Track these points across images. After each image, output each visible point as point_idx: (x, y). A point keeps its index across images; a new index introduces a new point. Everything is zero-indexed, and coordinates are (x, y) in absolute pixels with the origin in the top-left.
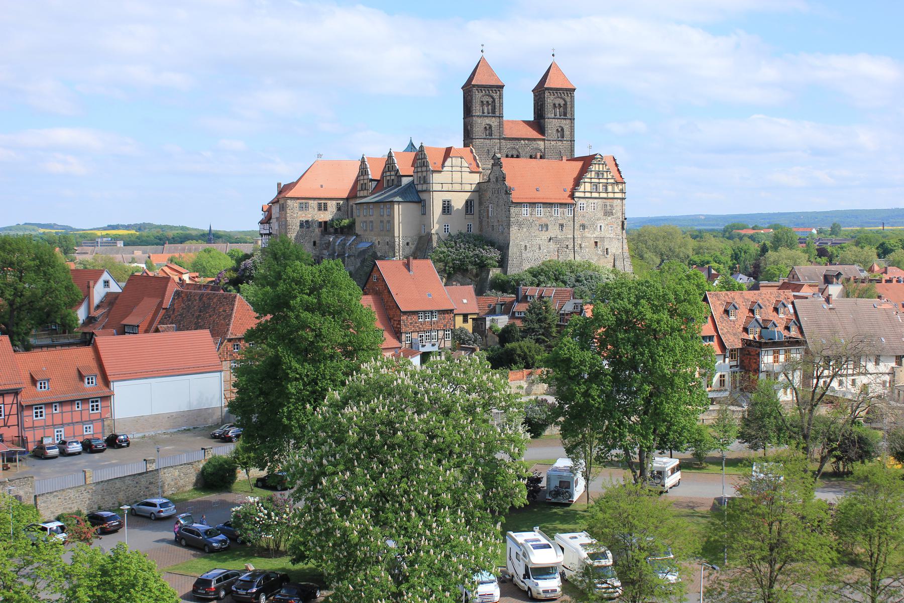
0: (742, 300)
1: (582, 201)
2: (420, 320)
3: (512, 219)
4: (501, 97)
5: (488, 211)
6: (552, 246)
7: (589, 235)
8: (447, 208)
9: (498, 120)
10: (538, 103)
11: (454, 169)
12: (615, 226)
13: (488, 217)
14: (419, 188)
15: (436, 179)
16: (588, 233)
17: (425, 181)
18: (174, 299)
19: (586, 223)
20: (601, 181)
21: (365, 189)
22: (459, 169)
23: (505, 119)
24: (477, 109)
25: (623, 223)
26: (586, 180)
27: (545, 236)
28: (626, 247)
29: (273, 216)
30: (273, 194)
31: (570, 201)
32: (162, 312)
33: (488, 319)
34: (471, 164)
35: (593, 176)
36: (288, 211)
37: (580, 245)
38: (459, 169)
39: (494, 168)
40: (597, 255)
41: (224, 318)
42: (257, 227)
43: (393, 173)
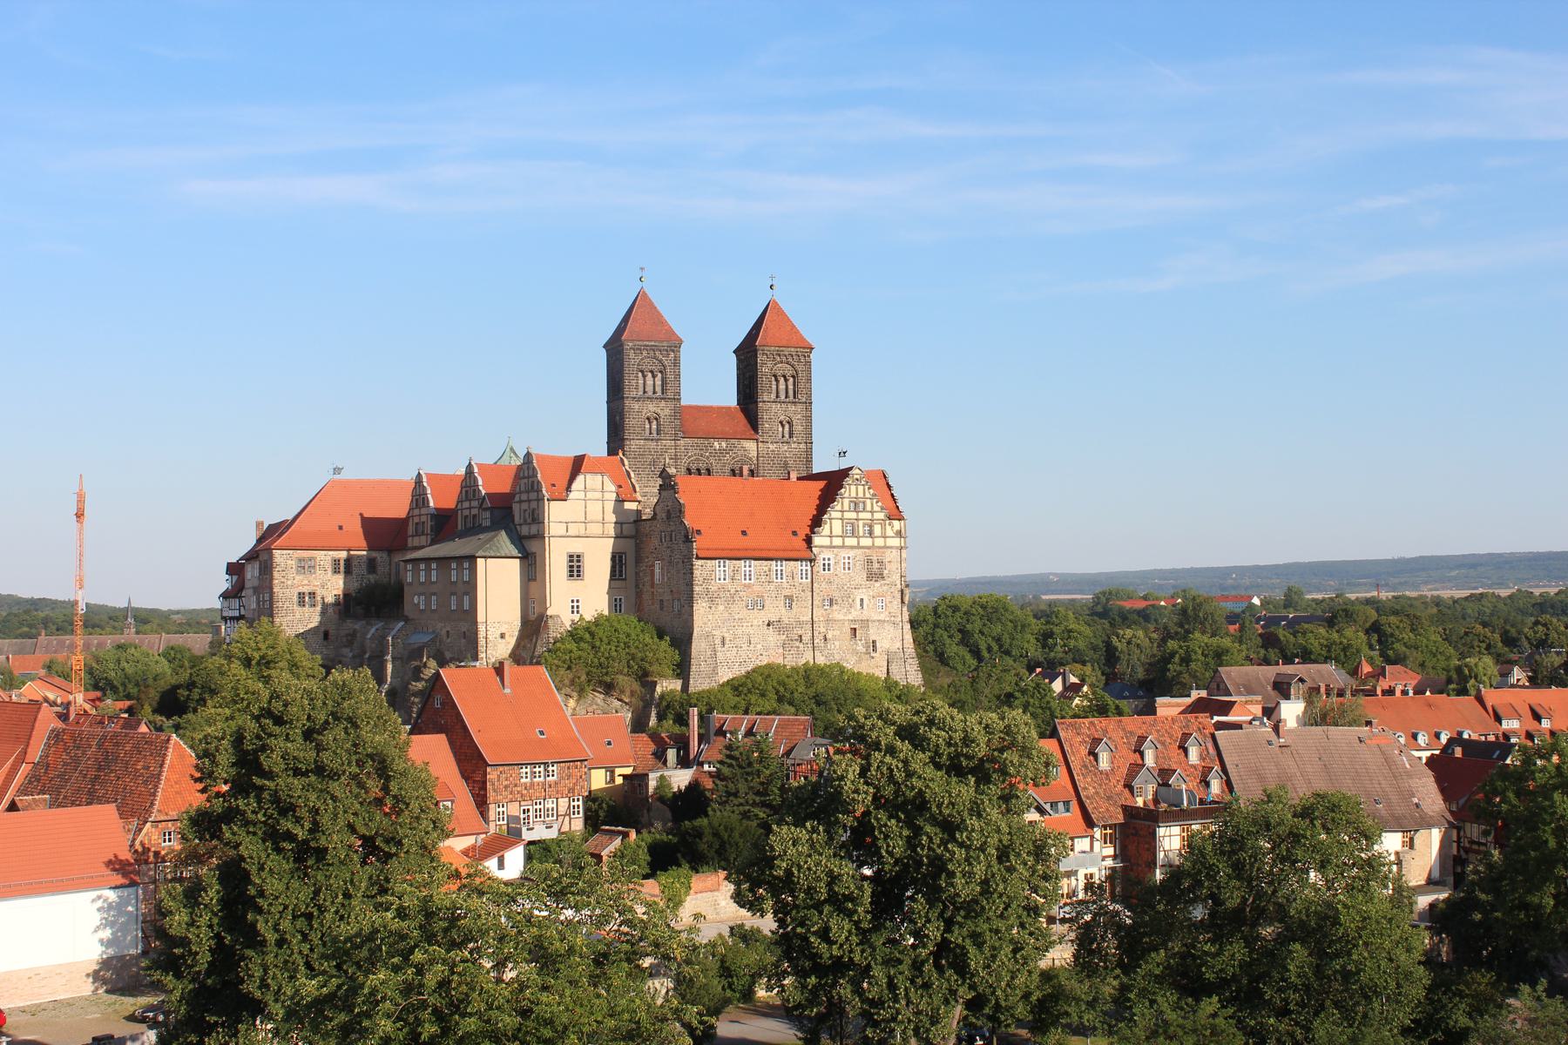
0: (1121, 733)
1: (826, 554)
2: (523, 780)
3: (697, 589)
4: (676, 363)
5: (653, 571)
6: (773, 638)
7: (841, 617)
8: (575, 567)
9: (671, 404)
10: (744, 374)
11: (590, 495)
12: (889, 599)
13: (653, 585)
14: (524, 530)
15: (556, 514)
16: (838, 613)
17: (537, 518)
18: (48, 745)
19: (836, 595)
20: (862, 515)
21: (423, 534)
22: (598, 495)
23: (683, 402)
24: (635, 384)
25: (902, 591)
26: (834, 514)
27: (760, 617)
28: (909, 637)
29: (248, 584)
30: (247, 542)
31: (807, 554)
32: (24, 769)
33: (651, 776)
34: (620, 487)
35: (846, 508)
36: (276, 574)
38: (598, 495)
39: (664, 493)
41: (145, 783)
42: (217, 604)
43: (475, 503)
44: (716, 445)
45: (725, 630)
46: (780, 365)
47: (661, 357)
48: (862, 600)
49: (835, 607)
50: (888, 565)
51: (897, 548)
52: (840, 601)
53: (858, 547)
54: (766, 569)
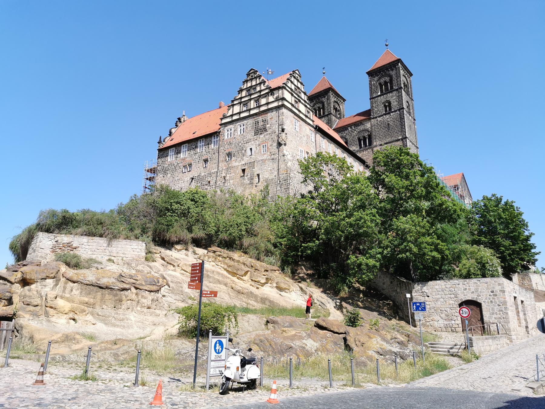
7: (237, 164)
19: (233, 150)
37: (225, 178)
48: (251, 149)
49: (233, 158)
50: (270, 123)
52: (236, 154)
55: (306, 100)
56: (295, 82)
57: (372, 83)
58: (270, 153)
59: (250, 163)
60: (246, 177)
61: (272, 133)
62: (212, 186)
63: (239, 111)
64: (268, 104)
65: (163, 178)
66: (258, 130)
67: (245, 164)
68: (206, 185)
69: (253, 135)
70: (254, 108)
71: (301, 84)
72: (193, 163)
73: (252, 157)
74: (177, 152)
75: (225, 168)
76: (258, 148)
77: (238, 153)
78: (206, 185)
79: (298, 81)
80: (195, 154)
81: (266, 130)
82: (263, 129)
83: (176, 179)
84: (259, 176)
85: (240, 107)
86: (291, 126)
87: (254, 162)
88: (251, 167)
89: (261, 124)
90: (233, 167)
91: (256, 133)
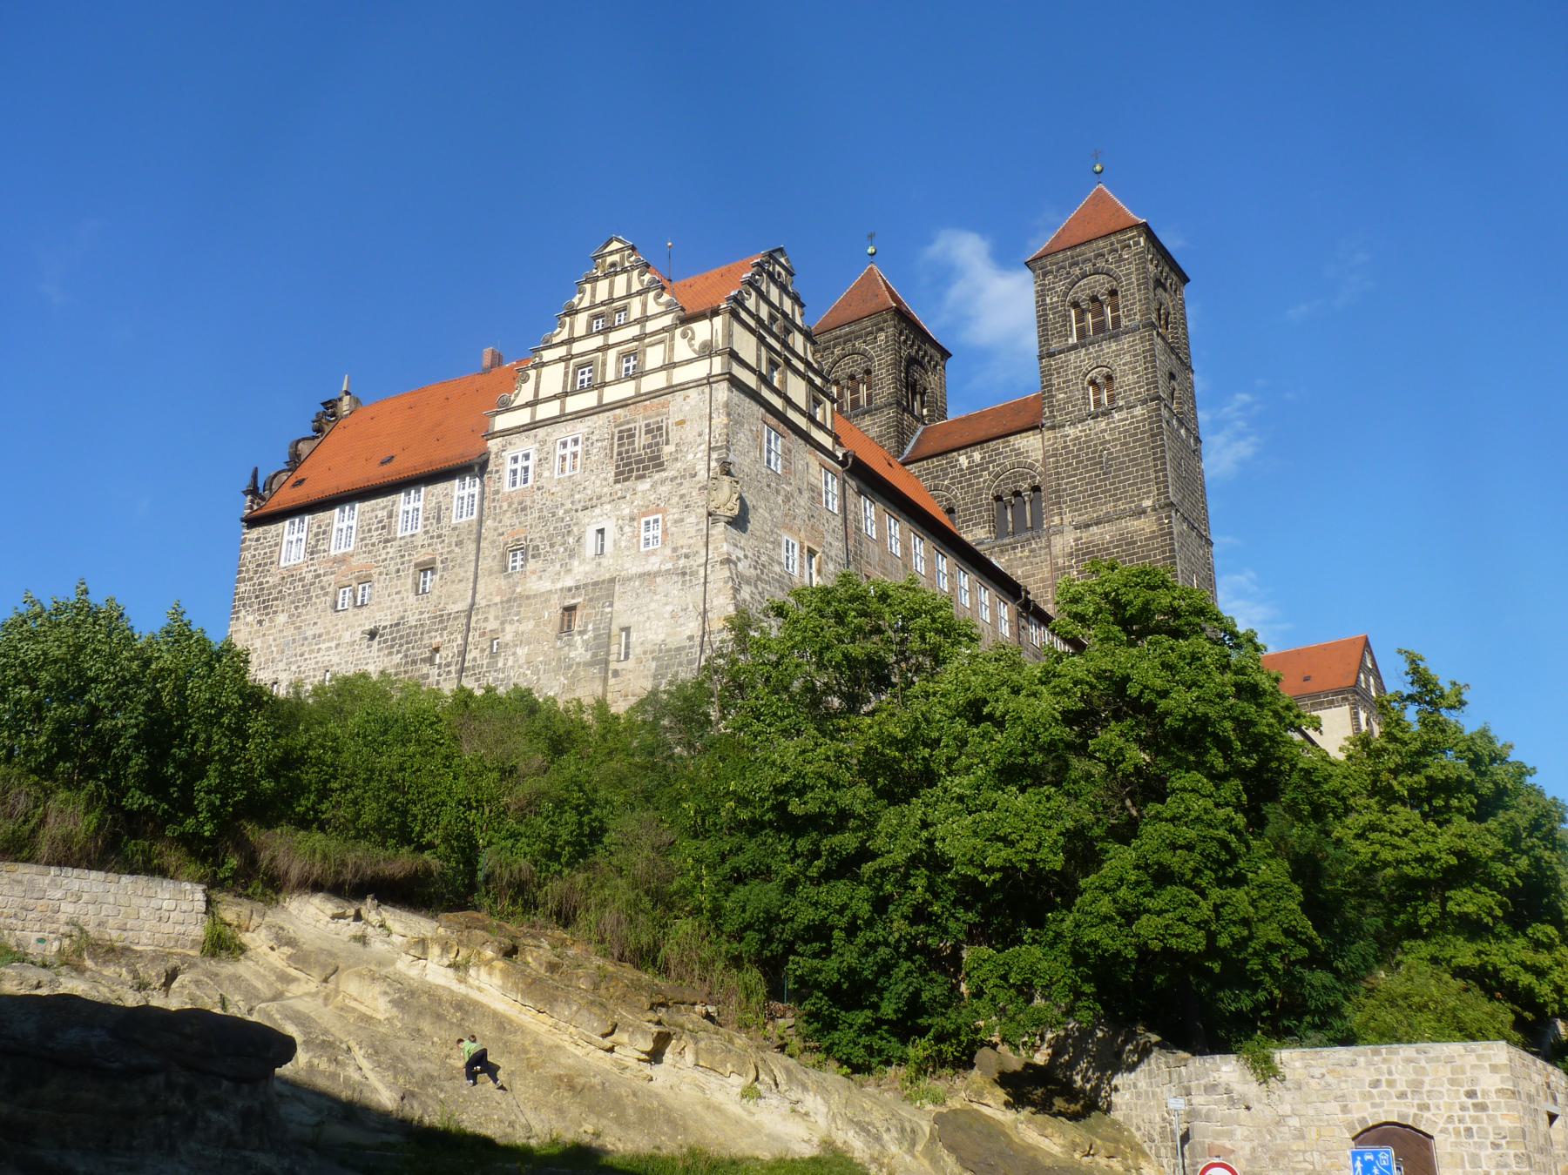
1: (522, 444)
7: (546, 585)
12: (674, 514)
19: (537, 534)
26: (548, 355)
40: (565, 665)
44: (963, 461)
45: (281, 666)
46: (1085, 281)
47: (863, 346)
48: (601, 531)
49: (532, 564)
50: (674, 436)
51: (698, 384)
52: (544, 547)
53: (601, 408)
54: (382, 514)
55: (810, 358)
56: (774, 295)
57: (1048, 301)
58: (675, 550)
59: (595, 584)
60: (577, 638)
61: (683, 477)
62: (448, 665)
63: (560, 390)
64: (669, 366)
65: (256, 627)
66: (631, 463)
67: (577, 588)
68: (424, 661)
69: (611, 477)
70: (618, 381)
71: (796, 299)
72: (375, 577)
73: (605, 561)
74: (315, 530)
75: (497, 599)
76: (627, 529)
77: (552, 546)
78: (424, 661)
79: (783, 288)
80: (387, 541)
81: (660, 466)
82: (651, 459)
83: (309, 633)
84: (628, 636)
85: (566, 374)
86: (755, 454)
87: (612, 580)
88: (598, 599)
89: (642, 440)
90: (528, 597)
91: (622, 473)
